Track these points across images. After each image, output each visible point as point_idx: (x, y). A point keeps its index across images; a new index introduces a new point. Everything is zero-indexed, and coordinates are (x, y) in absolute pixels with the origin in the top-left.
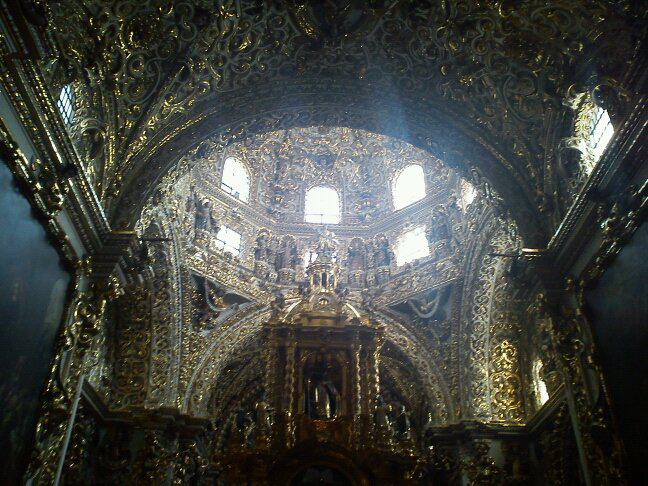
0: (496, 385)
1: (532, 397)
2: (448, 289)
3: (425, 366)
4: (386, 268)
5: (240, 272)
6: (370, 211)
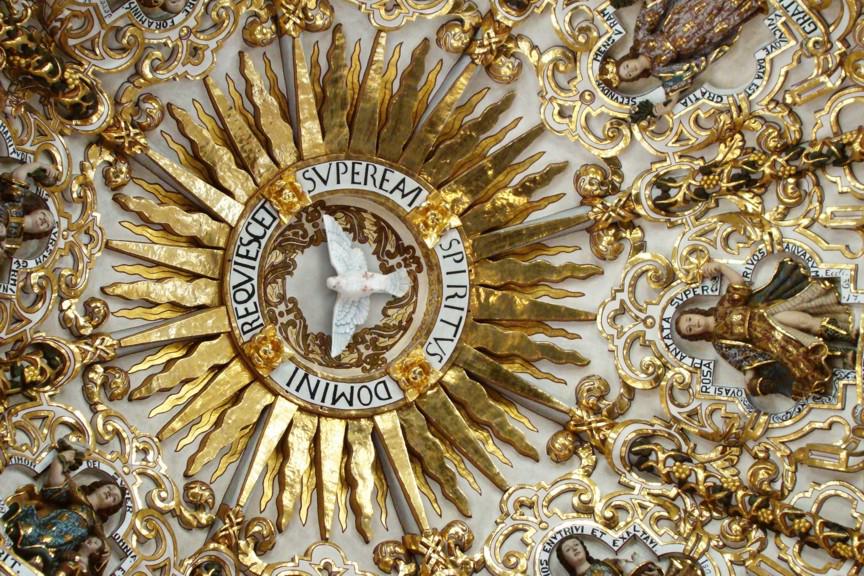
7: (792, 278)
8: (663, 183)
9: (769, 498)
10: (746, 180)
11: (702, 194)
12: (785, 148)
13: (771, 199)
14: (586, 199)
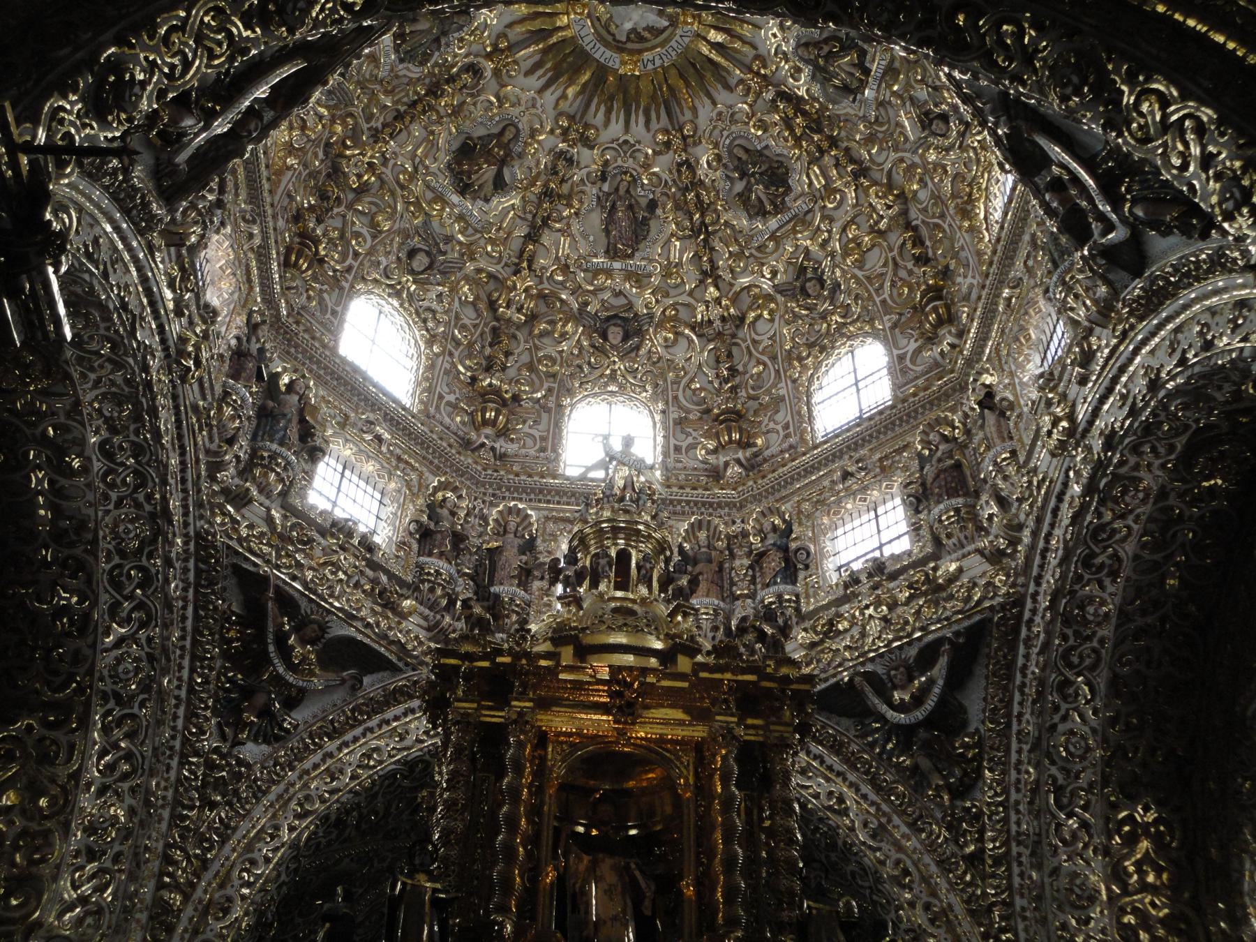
3: (906, 872)
4: (787, 592)
5: (375, 582)
6: (740, 455)
7: (500, 185)
8: (570, 161)
9: (424, 112)
10: (547, 194)
11: (556, 173)
12: (549, 217)
13: (533, 198)
14: (587, 126)
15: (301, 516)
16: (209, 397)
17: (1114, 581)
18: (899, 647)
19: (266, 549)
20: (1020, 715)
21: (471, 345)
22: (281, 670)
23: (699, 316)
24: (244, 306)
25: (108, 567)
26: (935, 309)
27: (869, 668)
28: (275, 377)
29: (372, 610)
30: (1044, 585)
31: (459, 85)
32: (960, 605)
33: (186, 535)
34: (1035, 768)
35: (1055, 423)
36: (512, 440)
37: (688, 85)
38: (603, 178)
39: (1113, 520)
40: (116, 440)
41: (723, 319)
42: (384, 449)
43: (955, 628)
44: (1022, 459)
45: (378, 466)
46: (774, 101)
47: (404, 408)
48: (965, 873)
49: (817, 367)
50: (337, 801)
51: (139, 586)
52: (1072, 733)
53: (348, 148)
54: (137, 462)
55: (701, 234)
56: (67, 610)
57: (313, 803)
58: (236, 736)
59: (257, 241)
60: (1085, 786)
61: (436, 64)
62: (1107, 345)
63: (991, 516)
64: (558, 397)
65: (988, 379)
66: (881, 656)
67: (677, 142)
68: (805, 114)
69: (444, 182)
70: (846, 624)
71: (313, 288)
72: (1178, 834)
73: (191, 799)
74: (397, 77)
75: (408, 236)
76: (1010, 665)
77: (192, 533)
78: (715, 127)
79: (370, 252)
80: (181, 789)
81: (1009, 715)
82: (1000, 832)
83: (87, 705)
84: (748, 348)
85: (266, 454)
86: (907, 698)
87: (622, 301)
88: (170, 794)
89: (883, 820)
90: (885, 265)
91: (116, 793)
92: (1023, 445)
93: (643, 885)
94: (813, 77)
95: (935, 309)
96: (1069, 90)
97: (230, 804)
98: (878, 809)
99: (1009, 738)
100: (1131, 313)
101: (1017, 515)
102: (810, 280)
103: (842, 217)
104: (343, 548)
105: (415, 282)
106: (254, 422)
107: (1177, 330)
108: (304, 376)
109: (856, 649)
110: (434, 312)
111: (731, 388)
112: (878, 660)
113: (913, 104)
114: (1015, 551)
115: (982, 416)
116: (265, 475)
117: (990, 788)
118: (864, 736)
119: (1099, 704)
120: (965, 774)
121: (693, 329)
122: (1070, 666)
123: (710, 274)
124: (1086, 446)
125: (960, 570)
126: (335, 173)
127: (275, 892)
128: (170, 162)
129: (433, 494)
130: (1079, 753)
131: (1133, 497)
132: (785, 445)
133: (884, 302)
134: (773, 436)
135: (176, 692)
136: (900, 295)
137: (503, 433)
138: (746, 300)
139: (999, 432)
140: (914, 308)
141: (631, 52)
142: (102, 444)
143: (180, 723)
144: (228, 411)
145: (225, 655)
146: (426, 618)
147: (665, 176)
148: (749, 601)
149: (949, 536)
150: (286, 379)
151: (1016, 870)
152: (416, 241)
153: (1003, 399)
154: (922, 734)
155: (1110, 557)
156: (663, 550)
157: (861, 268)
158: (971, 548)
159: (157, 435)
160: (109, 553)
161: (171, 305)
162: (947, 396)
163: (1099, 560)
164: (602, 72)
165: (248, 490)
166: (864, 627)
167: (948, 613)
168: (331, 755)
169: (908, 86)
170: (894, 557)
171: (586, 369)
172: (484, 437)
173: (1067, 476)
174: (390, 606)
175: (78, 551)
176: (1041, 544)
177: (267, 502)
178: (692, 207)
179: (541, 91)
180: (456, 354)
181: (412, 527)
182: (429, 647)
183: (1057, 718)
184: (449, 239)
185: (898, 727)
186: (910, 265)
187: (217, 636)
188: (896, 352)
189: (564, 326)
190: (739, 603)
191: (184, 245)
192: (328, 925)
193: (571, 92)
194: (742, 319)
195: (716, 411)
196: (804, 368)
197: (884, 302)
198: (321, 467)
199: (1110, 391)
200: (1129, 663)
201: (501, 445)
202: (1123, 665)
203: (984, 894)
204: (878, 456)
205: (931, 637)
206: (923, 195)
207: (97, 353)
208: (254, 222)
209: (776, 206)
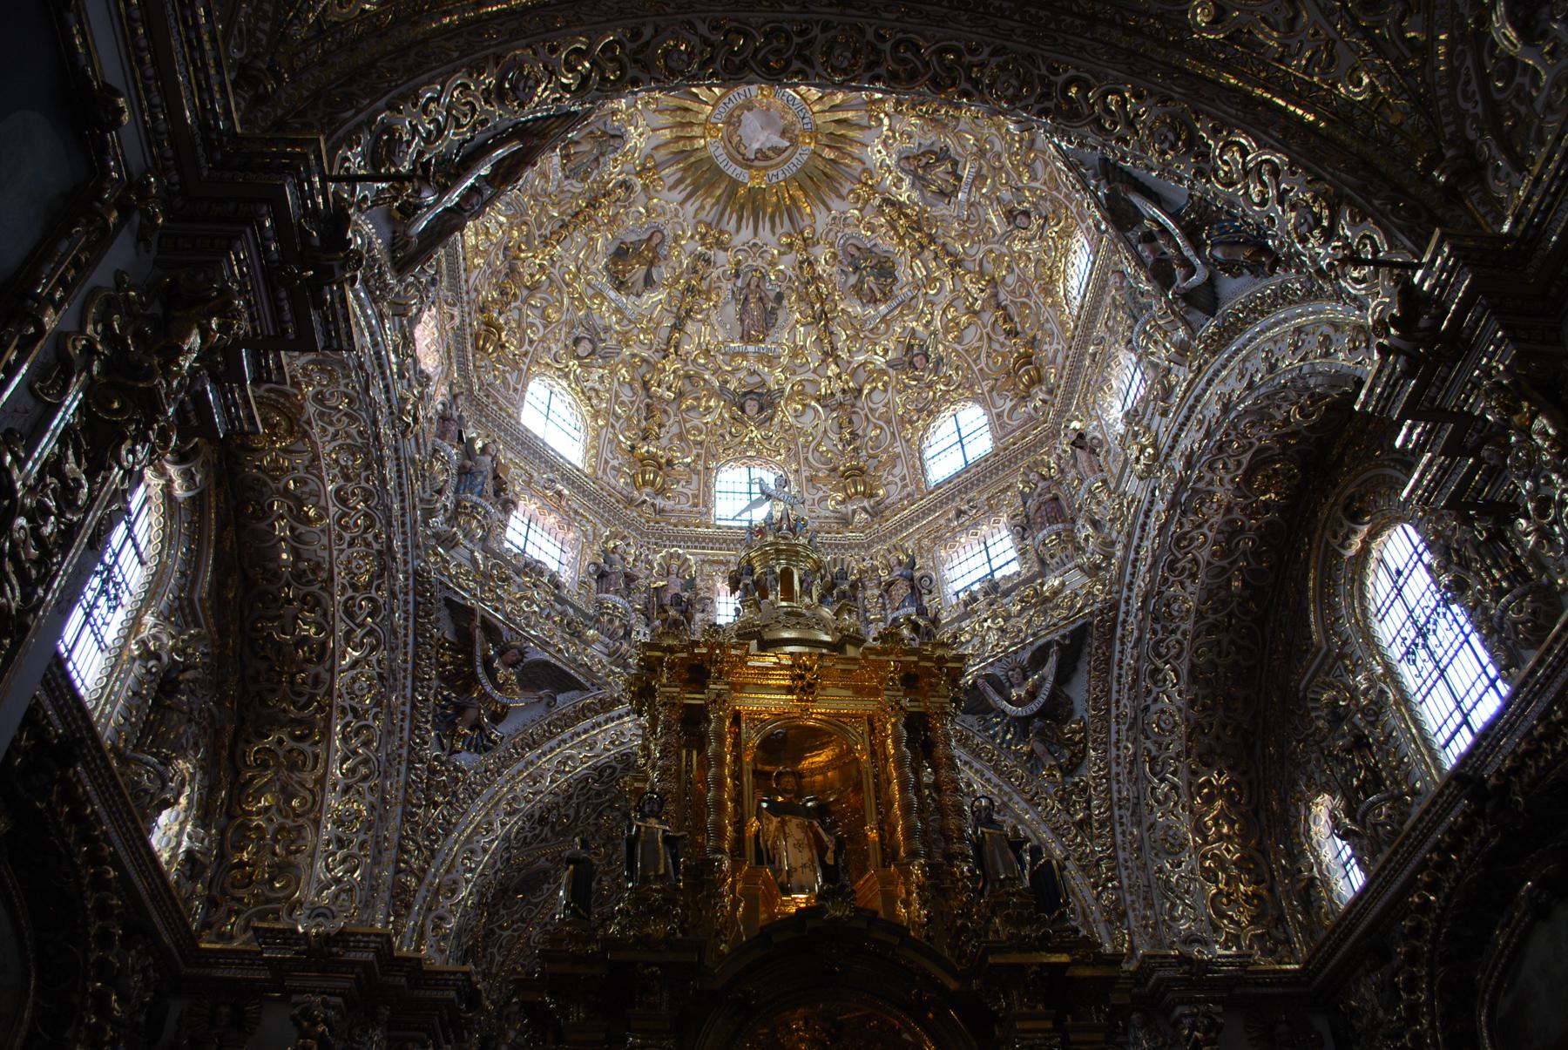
0: (1210, 876)
1: (1311, 889)
2: (1079, 636)
5: (563, 614)
7: (649, 282)
8: (708, 261)
9: (585, 221)
10: (690, 289)
12: (691, 310)
14: (722, 232)
15: (499, 556)
16: (423, 452)
17: (1193, 582)
18: (1015, 652)
19: (472, 585)
20: (1118, 701)
21: (629, 418)
22: (489, 688)
23: (823, 390)
24: (446, 378)
25: (343, 598)
26: (1027, 372)
27: (989, 671)
28: (472, 441)
29: (562, 637)
30: (1136, 590)
31: (613, 198)
32: (1065, 613)
33: (406, 572)
34: (1133, 743)
35: (1142, 451)
36: (669, 498)
37: (806, 195)
38: (737, 275)
39: (1193, 530)
40: (350, 487)
41: (844, 391)
42: (564, 503)
43: (1062, 632)
44: (1112, 486)
45: (559, 518)
46: (880, 206)
47: (578, 470)
48: (1076, 836)
49: (926, 428)
50: (540, 801)
51: (369, 615)
52: (1163, 711)
53: (522, 251)
54: (368, 506)
55: (822, 319)
56: (305, 640)
57: (520, 803)
58: (452, 745)
59: (457, 321)
60: (1173, 755)
61: (595, 180)
62: (1184, 380)
63: (1086, 539)
64: (705, 462)
65: (1076, 424)
66: (1000, 660)
67: (799, 243)
68: (906, 216)
69: (603, 280)
70: (968, 636)
71: (498, 369)
72: (1246, 792)
73: (418, 799)
74: (562, 192)
75: (573, 327)
76: (1108, 660)
77: (411, 571)
78: (830, 230)
79: (542, 340)
80: (410, 791)
81: (1108, 703)
82: (1104, 800)
83: (328, 721)
84: (866, 415)
85: (468, 505)
86: (1023, 694)
87: (756, 379)
88: (401, 794)
89: (1005, 799)
90: (980, 339)
91: (358, 792)
92: (1113, 475)
93: (826, 839)
94: (913, 185)
95: (1027, 372)
96: (1166, 146)
97: (449, 803)
98: (1000, 790)
99: (1108, 722)
100: (1205, 349)
101: (1110, 534)
102: (917, 355)
103: (943, 301)
104: (535, 586)
105: (580, 366)
106: (456, 479)
107: (1244, 360)
108: (494, 441)
109: (978, 655)
110: (597, 391)
111: (854, 449)
112: (997, 664)
113: (999, 203)
114: (1110, 564)
115: (1074, 456)
116: (469, 522)
117: (1095, 764)
118: (987, 729)
119: (1183, 686)
120: (1074, 755)
121: (818, 401)
122: (1159, 656)
123: (831, 354)
124: (1168, 468)
125: (1063, 584)
126: (512, 272)
127: (491, 877)
128: (405, 234)
129: (606, 542)
130: (1169, 727)
131: (1209, 508)
132: (904, 493)
133: (981, 370)
134: (892, 488)
135: (402, 708)
136: (995, 363)
137: (661, 492)
138: (862, 375)
139: (1091, 467)
140: (1008, 374)
141: (758, 169)
142: (337, 491)
143: (406, 734)
144: (438, 466)
145: (441, 677)
146: (606, 646)
147: (789, 272)
148: (881, 624)
149: (1052, 556)
150: (479, 444)
151: (1118, 829)
152: (580, 332)
153: (1094, 438)
154: (1037, 723)
155: (1190, 562)
156: (819, 568)
157: (959, 343)
158: (1069, 566)
159: (383, 482)
160: (344, 588)
161: (395, 368)
162: (1042, 444)
163: (1179, 565)
164: (735, 184)
165: (455, 533)
166: (983, 638)
167: (1055, 620)
168: (532, 763)
169: (994, 188)
170: (1005, 578)
171: (728, 438)
172: (645, 494)
173: (1154, 495)
174: (577, 635)
175: (315, 588)
176: (1132, 555)
177: (470, 546)
178: (813, 298)
179: (682, 204)
180: (617, 426)
181: (592, 569)
182: (611, 670)
183: (1149, 700)
184: (607, 329)
185: (1016, 719)
186: (1002, 339)
187: (433, 660)
188: (994, 411)
189: (708, 401)
190: (873, 625)
191: (404, 315)
192: (571, 867)
193: (710, 201)
194: (860, 391)
195: (842, 468)
196: (916, 429)
197: (981, 370)
198: (512, 521)
199: (1187, 418)
200: (1203, 654)
201: (660, 502)
202: (1199, 657)
203: (1093, 851)
204: (985, 496)
205: (1041, 642)
206: (1010, 279)
207: (336, 408)
208: (454, 305)
209: (885, 294)
